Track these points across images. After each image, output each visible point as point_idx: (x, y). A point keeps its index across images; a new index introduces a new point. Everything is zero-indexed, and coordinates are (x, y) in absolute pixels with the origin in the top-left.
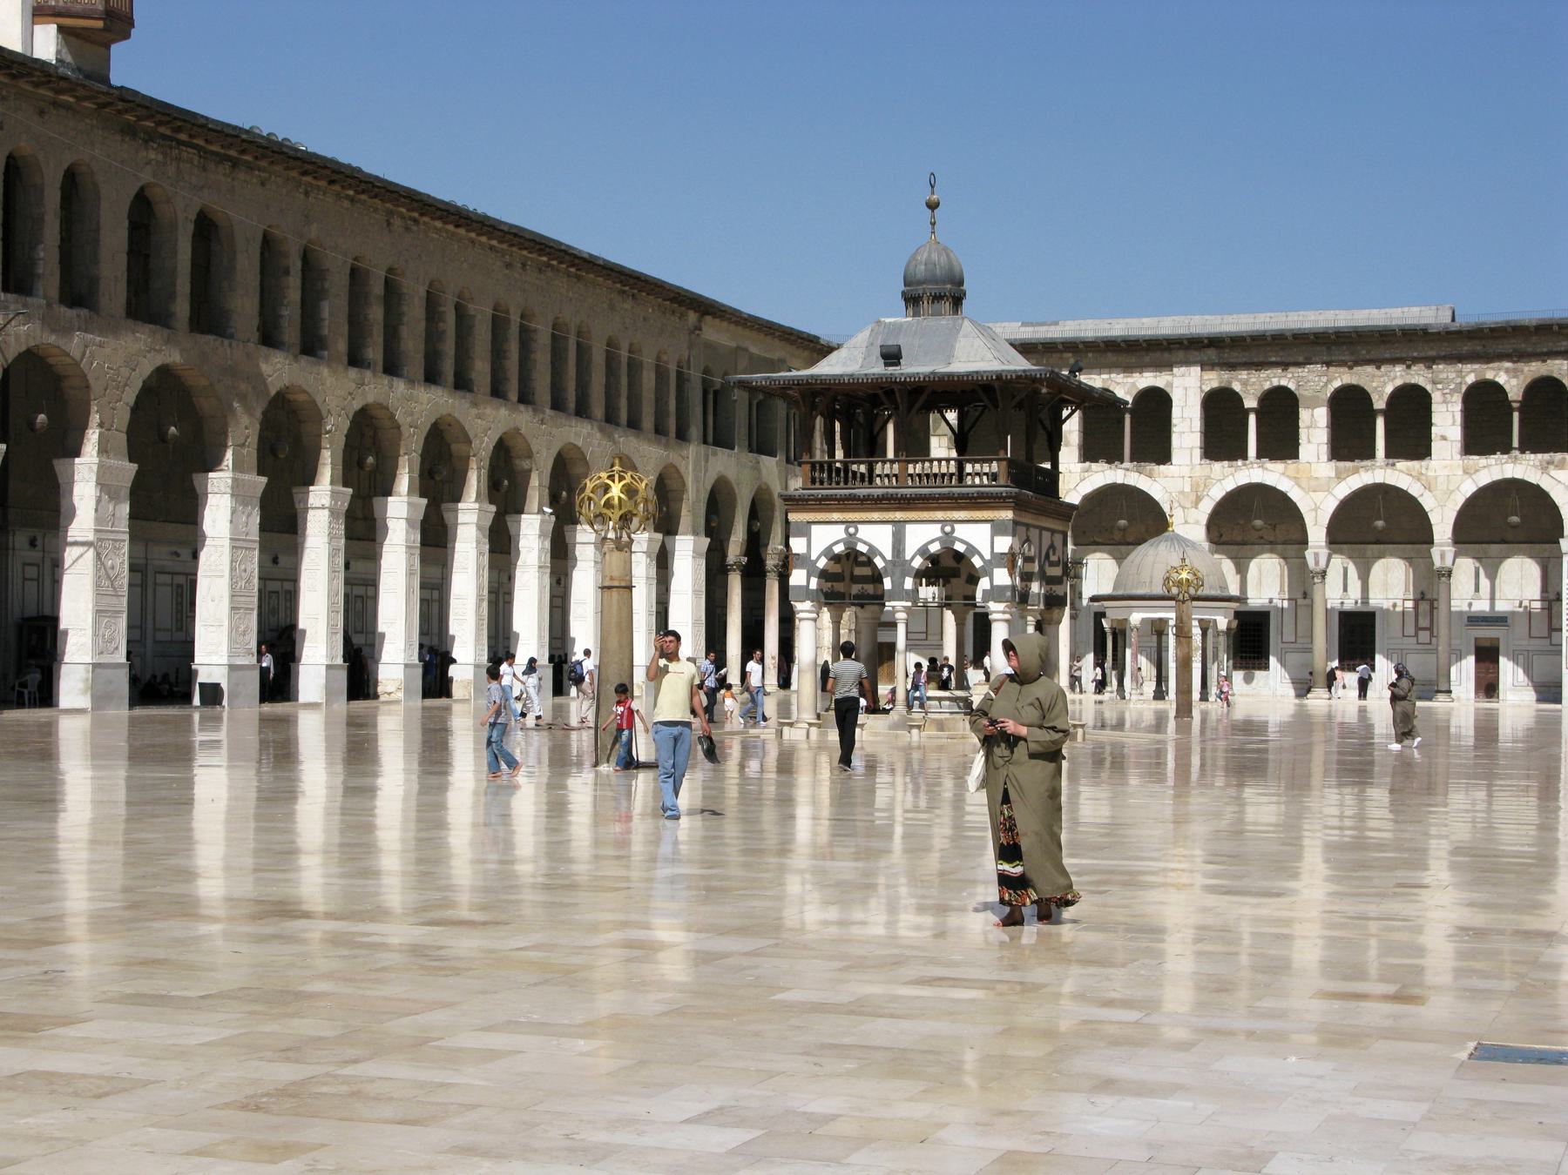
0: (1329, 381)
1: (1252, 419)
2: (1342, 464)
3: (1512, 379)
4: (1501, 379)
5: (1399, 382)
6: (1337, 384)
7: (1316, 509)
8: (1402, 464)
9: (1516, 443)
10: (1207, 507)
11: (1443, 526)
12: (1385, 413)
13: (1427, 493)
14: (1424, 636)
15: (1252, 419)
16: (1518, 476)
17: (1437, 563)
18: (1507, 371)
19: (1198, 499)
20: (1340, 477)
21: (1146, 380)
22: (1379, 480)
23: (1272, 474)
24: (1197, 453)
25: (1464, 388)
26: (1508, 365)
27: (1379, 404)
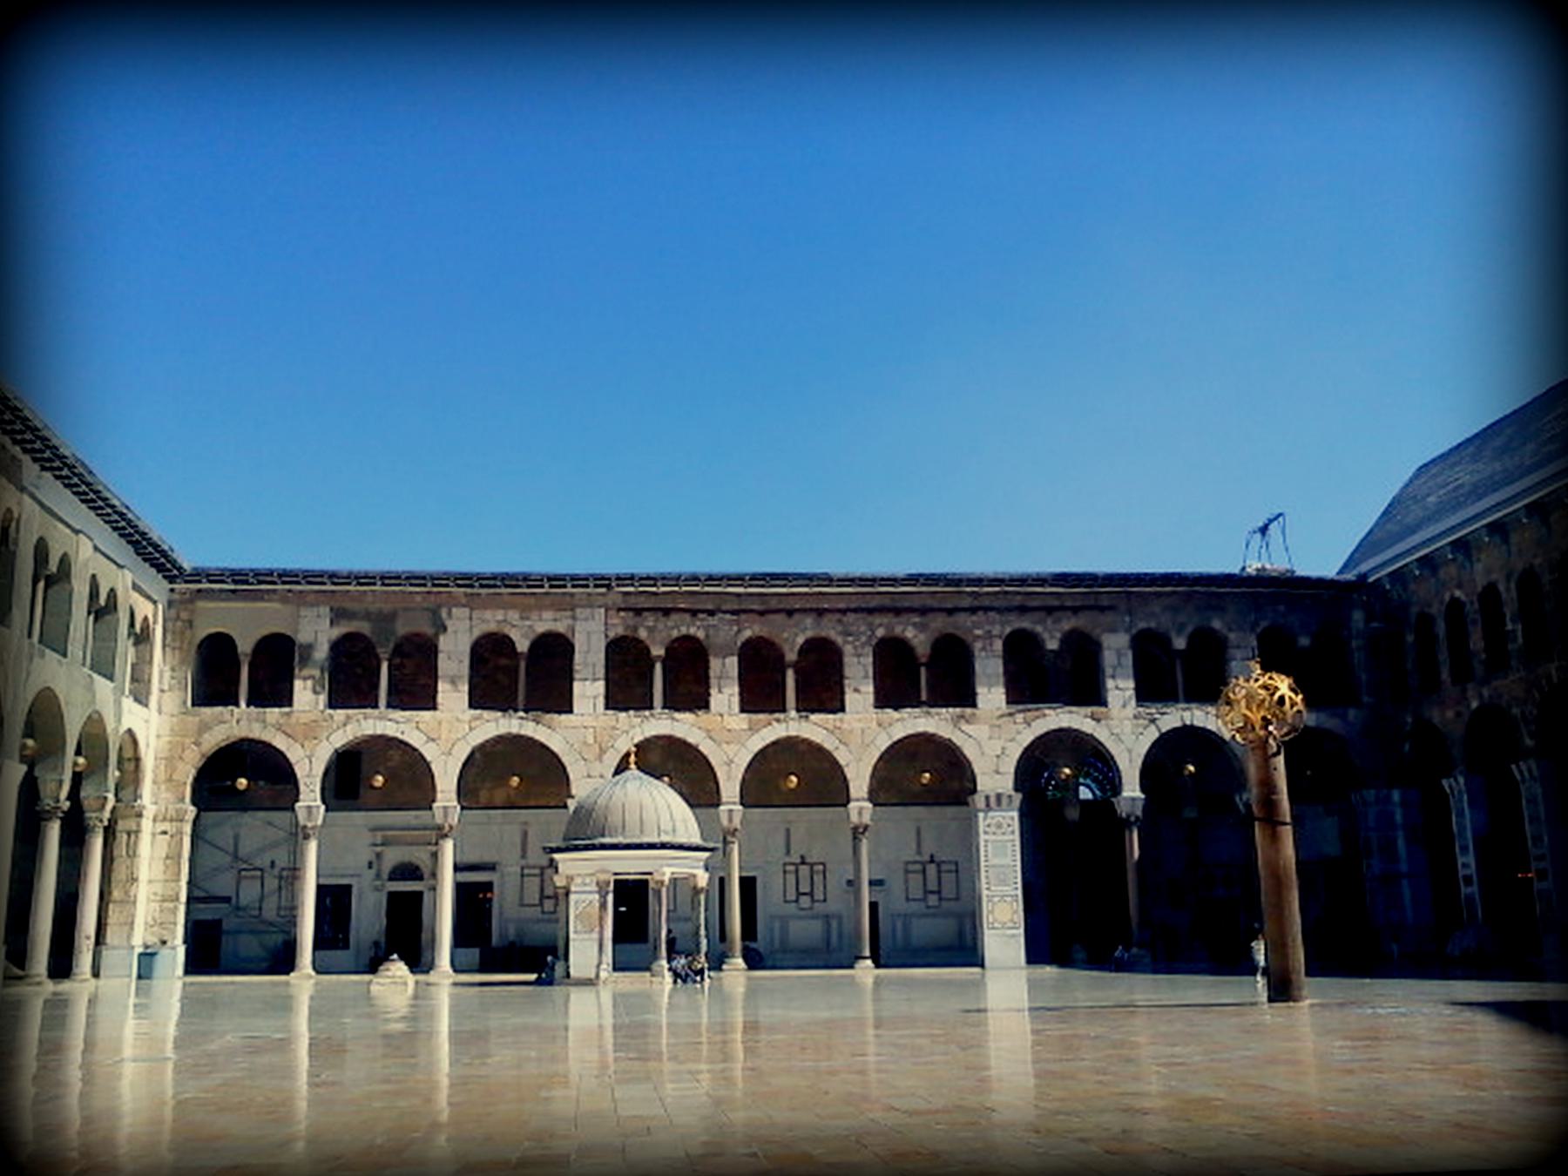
0: (739, 631)
1: (658, 668)
2: (754, 717)
3: (917, 637)
4: (910, 633)
5: (809, 634)
6: (748, 633)
7: (730, 763)
8: (814, 717)
9: (924, 697)
10: (613, 760)
11: (859, 781)
12: (796, 667)
13: (842, 747)
14: (805, 901)
15: (658, 668)
16: (931, 730)
17: (854, 818)
18: (914, 625)
19: (602, 751)
20: (753, 729)
21: (546, 622)
22: (793, 733)
23: (684, 726)
24: (601, 701)
25: (874, 642)
26: (917, 620)
27: (791, 656)
